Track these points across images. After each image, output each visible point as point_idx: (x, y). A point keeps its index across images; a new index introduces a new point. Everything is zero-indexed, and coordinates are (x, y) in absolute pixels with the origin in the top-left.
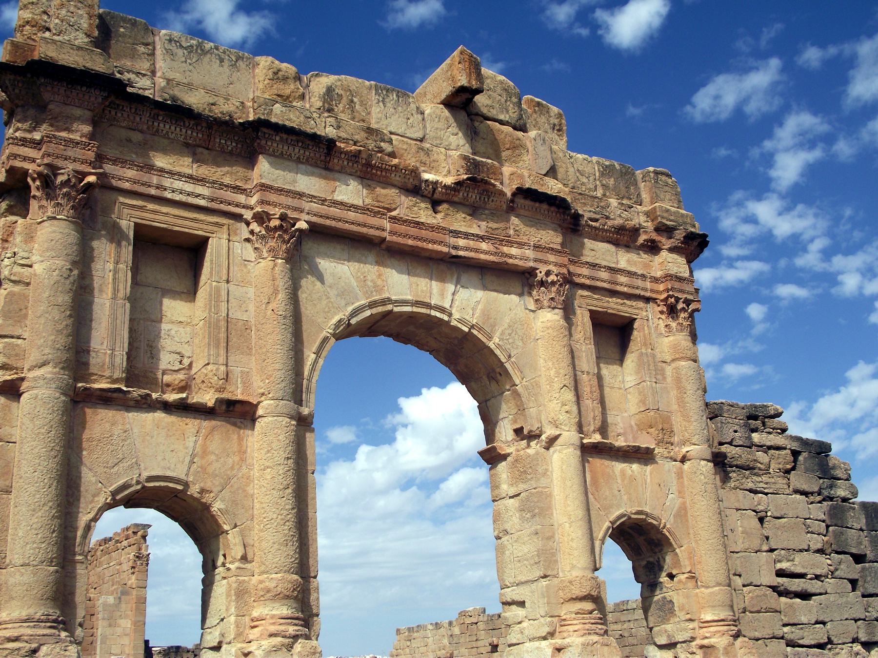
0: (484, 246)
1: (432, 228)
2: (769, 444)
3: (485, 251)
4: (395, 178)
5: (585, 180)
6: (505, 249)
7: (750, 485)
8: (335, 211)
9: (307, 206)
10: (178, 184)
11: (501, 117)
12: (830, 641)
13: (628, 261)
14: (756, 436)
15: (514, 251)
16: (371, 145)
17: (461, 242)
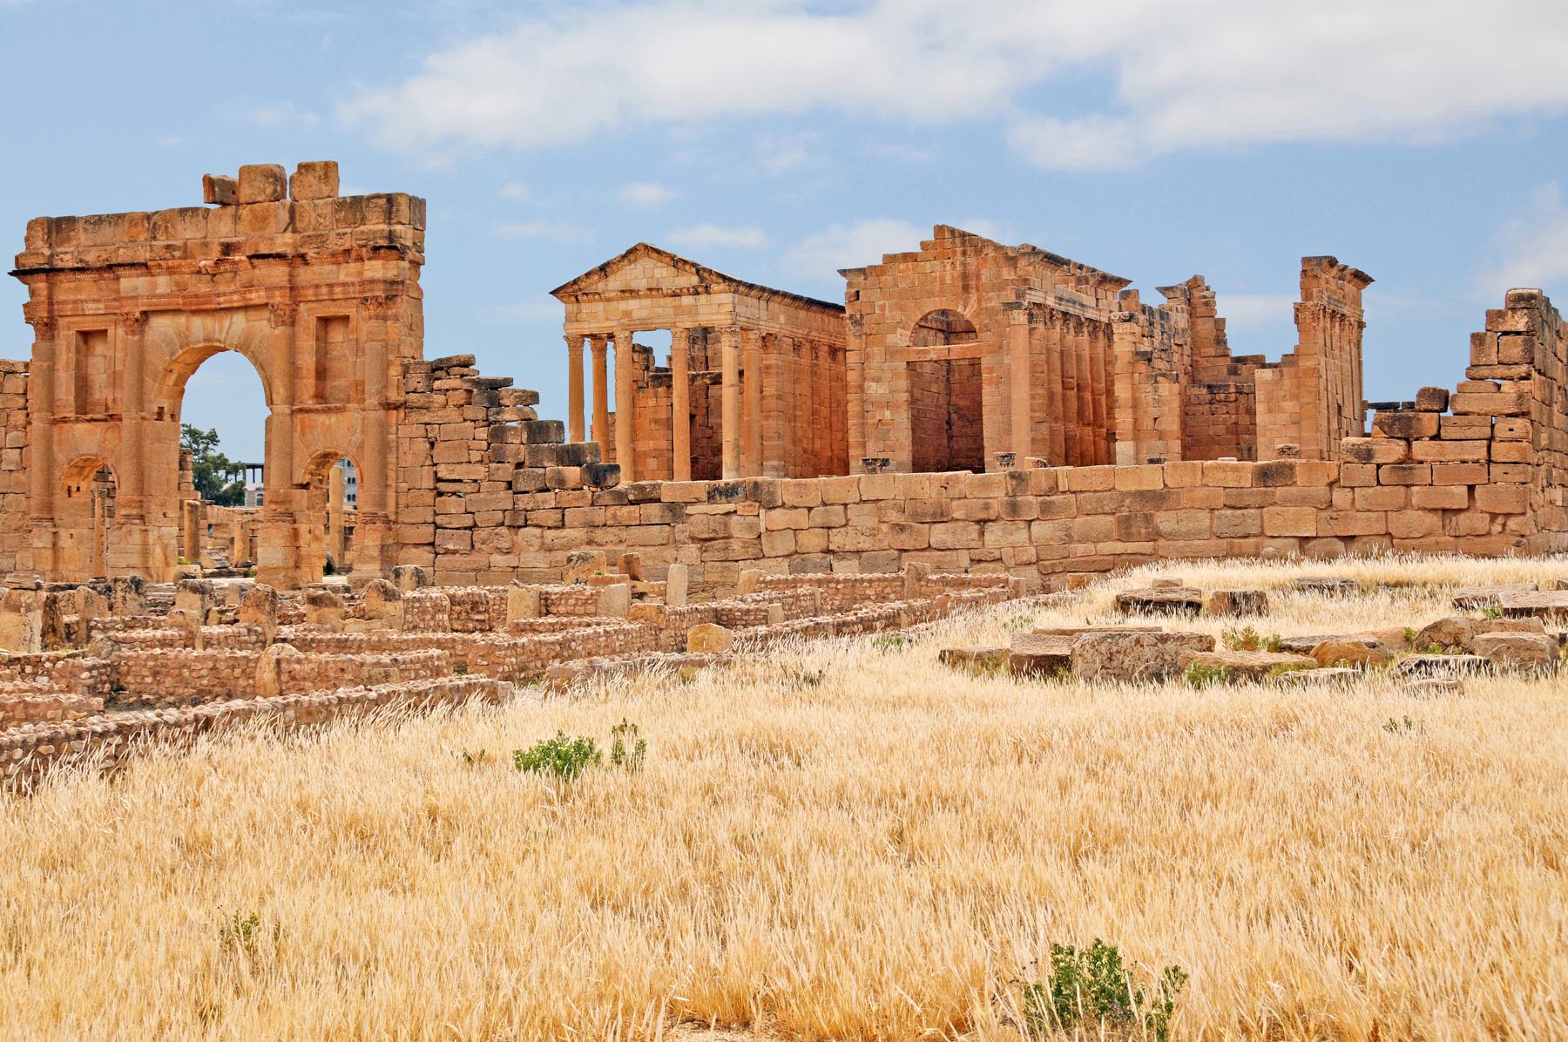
0: (235, 297)
1: (206, 295)
2: (446, 387)
3: (236, 300)
4: (185, 270)
5: (322, 220)
6: (248, 296)
7: (427, 419)
8: (155, 300)
9: (140, 302)
10: (90, 305)
11: (260, 199)
12: (475, 525)
13: (347, 275)
14: (437, 384)
15: (254, 295)
16: (168, 255)
17: (222, 299)
